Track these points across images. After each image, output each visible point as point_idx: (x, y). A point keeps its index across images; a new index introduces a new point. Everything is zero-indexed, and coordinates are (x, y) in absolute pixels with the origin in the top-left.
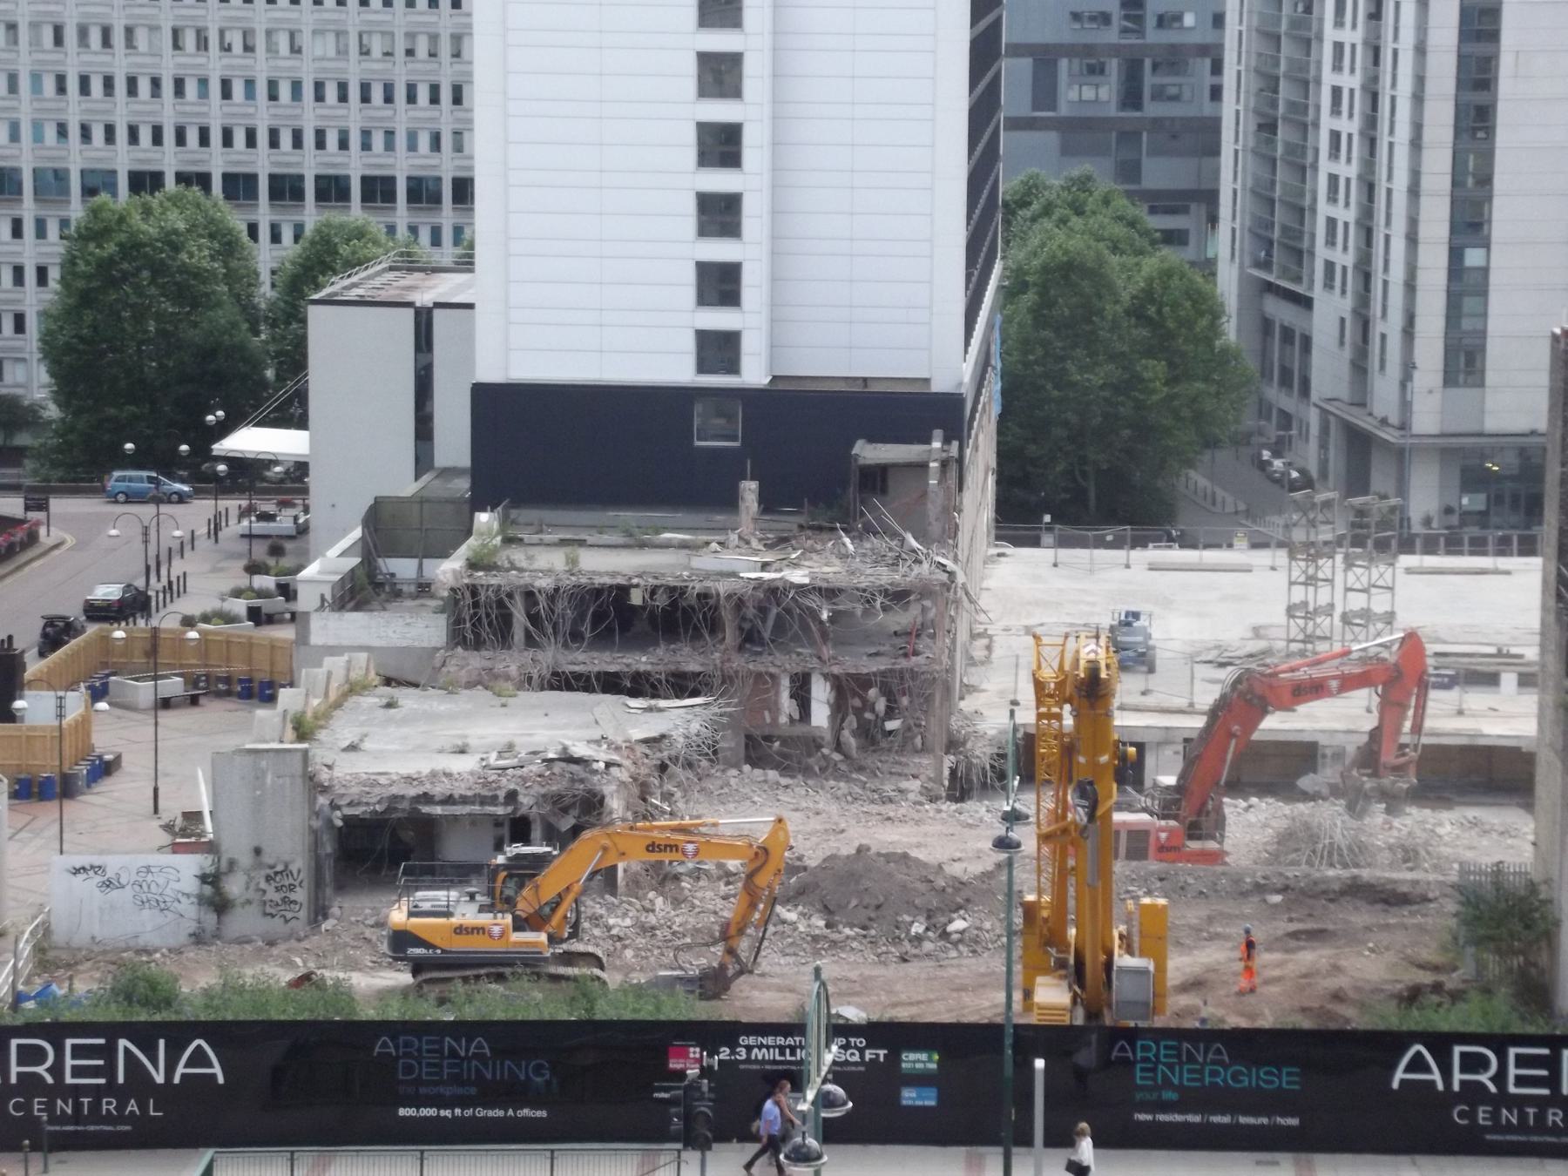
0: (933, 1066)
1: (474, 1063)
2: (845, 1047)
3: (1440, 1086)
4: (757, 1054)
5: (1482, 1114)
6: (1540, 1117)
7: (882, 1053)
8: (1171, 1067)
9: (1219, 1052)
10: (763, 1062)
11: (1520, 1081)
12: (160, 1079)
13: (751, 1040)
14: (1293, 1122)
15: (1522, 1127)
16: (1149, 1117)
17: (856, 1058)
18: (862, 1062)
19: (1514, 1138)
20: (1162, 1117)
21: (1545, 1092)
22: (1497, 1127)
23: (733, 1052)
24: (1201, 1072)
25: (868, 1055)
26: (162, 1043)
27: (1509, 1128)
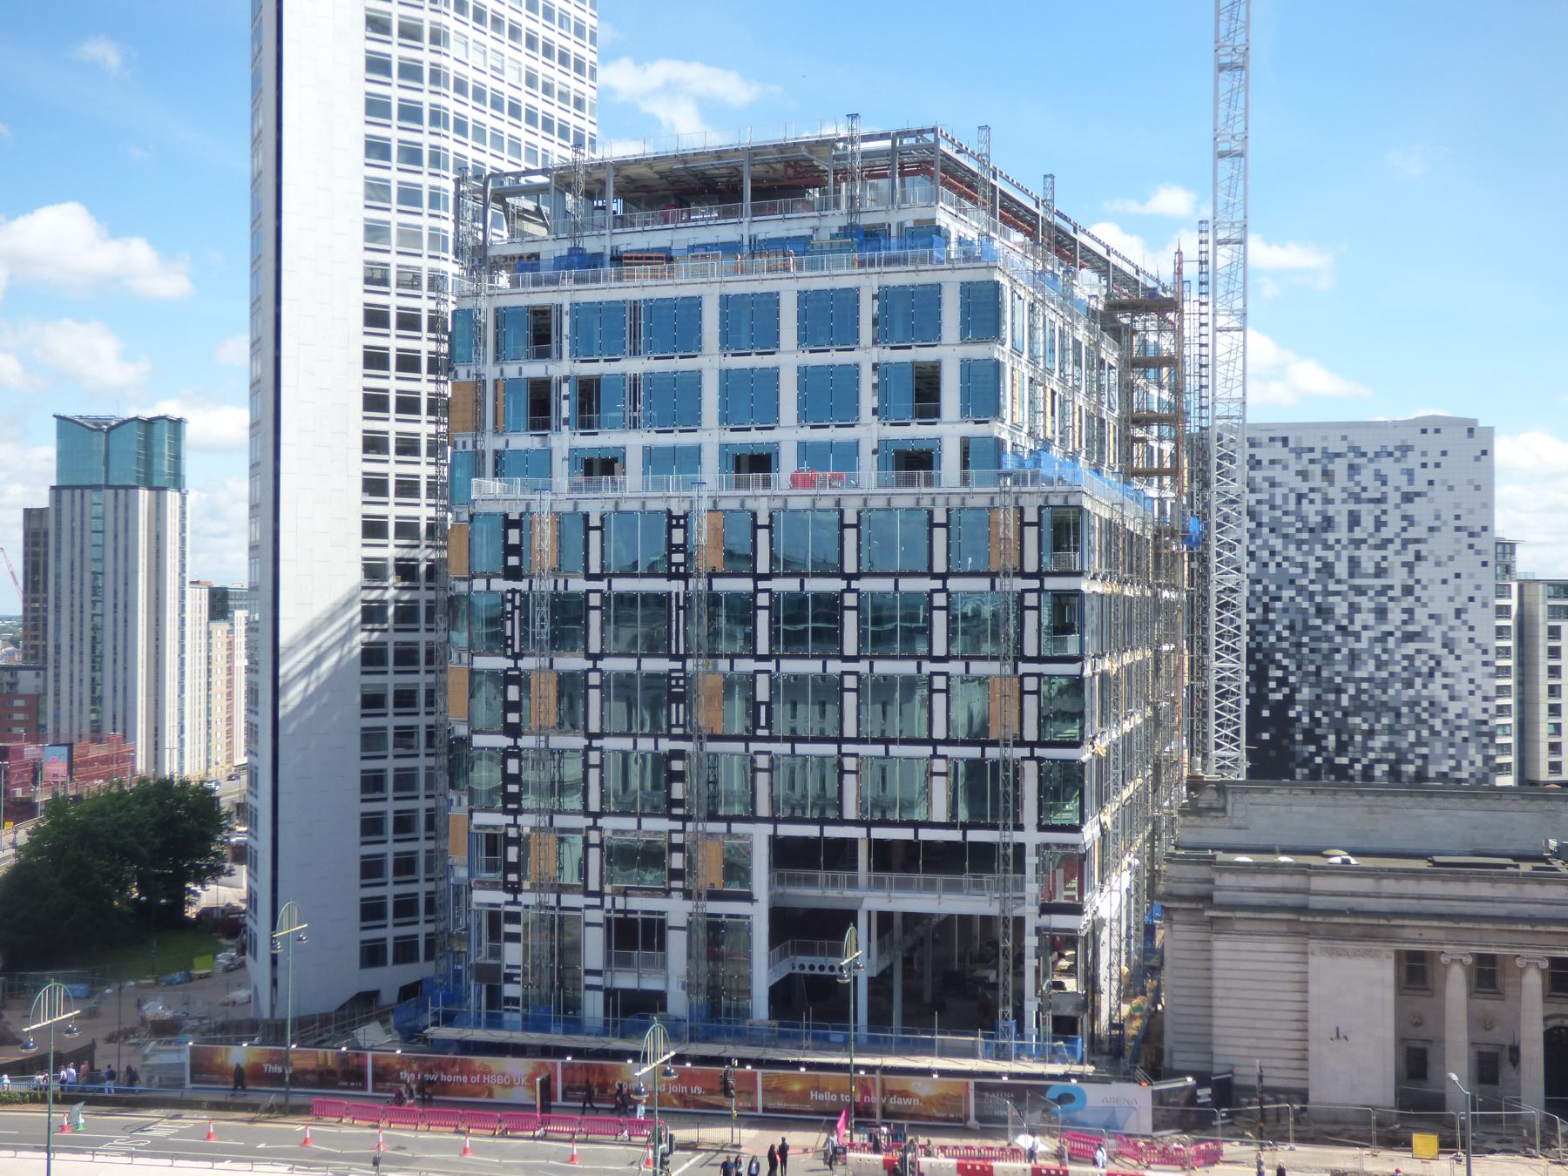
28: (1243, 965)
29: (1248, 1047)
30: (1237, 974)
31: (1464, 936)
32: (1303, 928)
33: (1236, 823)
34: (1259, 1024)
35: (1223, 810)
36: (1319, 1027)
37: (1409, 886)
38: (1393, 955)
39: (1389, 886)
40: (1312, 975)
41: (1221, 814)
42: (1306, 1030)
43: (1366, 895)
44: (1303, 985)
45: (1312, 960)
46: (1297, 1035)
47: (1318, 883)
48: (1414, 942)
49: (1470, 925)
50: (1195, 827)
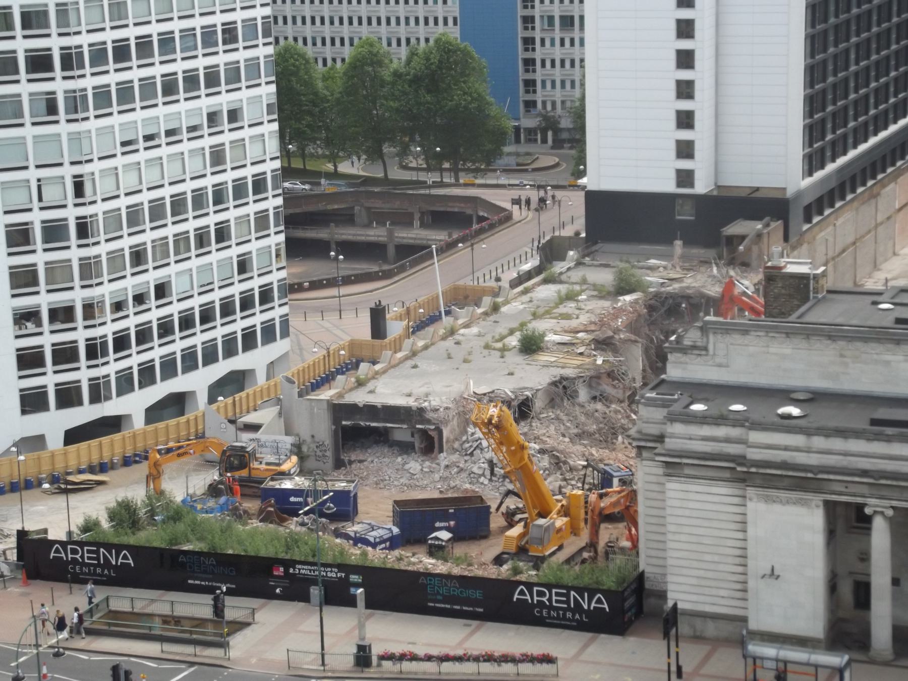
0: (360, 581)
1: (211, 567)
2: (331, 571)
3: (530, 601)
4: (303, 572)
5: (545, 612)
6: (564, 615)
7: (343, 575)
8: (438, 587)
9: (455, 583)
10: (304, 574)
11: (557, 601)
12: (114, 563)
13: (300, 567)
14: (481, 610)
15: (558, 618)
16: (433, 605)
17: (335, 576)
18: (337, 577)
19: (555, 622)
20: (437, 605)
21: (565, 606)
22: (550, 617)
23: (294, 570)
24: (450, 590)
25: (339, 575)
26: (114, 551)
27: (554, 618)
28: (691, 505)
29: (698, 577)
30: (687, 513)
31: (885, 493)
32: (742, 476)
33: (718, 360)
34: (708, 557)
35: (706, 349)
36: (758, 564)
37: (837, 444)
38: (821, 504)
39: (819, 442)
40: (750, 518)
41: (704, 353)
42: (745, 566)
43: (797, 449)
44: (743, 527)
45: (749, 504)
46: (740, 569)
47: (756, 437)
48: (840, 494)
49: (889, 482)
50: (681, 363)
